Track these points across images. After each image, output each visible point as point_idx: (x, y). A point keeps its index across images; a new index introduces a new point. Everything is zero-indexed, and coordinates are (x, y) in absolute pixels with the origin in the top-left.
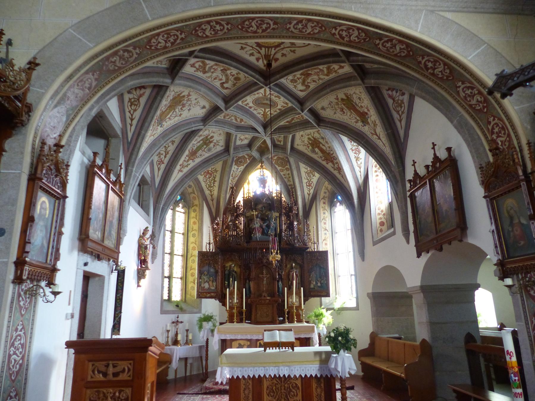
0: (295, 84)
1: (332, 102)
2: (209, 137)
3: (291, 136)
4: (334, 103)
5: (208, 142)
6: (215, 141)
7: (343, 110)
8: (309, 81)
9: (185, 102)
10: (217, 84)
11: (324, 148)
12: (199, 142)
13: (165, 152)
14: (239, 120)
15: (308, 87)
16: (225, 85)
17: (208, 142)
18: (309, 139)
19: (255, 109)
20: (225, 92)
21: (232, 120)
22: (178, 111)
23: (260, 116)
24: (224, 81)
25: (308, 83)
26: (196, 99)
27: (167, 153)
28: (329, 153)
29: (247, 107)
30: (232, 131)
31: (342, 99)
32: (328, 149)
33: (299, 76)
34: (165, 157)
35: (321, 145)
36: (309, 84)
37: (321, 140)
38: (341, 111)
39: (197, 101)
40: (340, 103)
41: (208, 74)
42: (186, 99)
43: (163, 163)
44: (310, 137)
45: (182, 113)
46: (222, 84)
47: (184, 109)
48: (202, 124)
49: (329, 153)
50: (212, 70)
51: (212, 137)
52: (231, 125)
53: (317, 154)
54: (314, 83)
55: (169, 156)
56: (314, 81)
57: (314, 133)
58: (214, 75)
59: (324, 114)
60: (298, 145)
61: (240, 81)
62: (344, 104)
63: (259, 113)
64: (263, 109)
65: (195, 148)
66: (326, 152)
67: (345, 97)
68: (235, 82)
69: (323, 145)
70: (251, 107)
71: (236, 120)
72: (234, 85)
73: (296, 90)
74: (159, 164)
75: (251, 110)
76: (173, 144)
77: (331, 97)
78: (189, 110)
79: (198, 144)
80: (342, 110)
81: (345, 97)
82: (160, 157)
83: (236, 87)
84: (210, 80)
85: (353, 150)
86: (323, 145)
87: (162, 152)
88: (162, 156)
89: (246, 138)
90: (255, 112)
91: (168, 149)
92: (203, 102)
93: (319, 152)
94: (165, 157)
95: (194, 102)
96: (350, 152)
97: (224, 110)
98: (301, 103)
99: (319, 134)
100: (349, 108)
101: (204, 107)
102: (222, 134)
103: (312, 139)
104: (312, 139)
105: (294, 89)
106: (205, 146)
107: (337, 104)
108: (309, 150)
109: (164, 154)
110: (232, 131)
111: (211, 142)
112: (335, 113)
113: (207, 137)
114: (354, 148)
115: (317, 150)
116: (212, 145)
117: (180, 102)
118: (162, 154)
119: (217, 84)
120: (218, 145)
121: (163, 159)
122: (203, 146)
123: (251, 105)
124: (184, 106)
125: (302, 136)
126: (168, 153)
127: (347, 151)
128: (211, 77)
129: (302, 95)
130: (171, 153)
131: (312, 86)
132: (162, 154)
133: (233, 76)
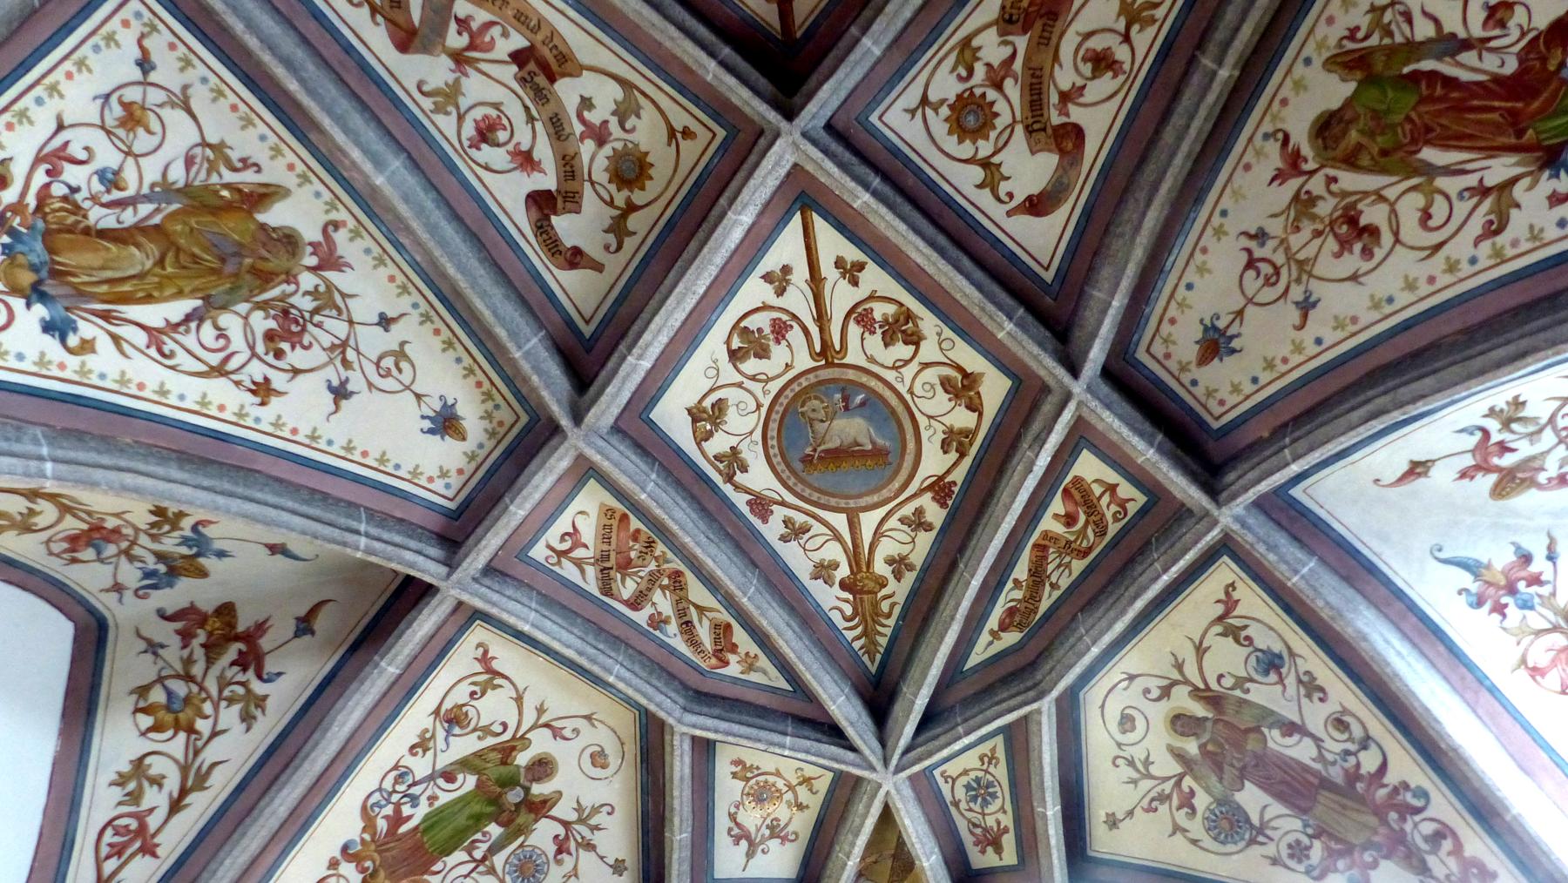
0: (985, 148)
1: (1261, 236)
2: (522, 759)
3: (1047, 706)
4: (1275, 227)
5: (514, 796)
6: (564, 810)
7: (1351, 219)
8: (1065, 78)
9: (307, 304)
10: (508, 193)
11: (1301, 751)
12: (449, 776)
13: (184, 769)
14: (704, 633)
15: (1069, 139)
16: (562, 224)
17: (514, 796)
18: (1180, 723)
19: (795, 532)
20: (578, 291)
21: (658, 621)
22: (238, 342)
23: (830, 599)
24: (547, 181)
25: (1065, 97)
26: (385, 322)
27: (193, 779)
28: (1354, 776)
29: (740, 501)
30: (666, 706)
31: (1327, 127)
32: (1334, 746)
33: (992, 49)
34: (176, 806)
35: (1276, 740)
36: (1076, 114)
37: (1263, 694)
38: (1345, 245)
39: (390, 340)
40: (1316, 185)
41: (436, 70)
42: (307, 281)
43: (149, 850)
44: (1182, 700)
45: (278, 380)
46: (542, 203)
47: (296, 357)
48: (434, 551)
49: (1354, 776)
50: (456, 40)
51: (543, 767)
52: (662, 668)
53: (1258, 833)
54: (1106, 84)
55: (201, 806)
56: (1102, 62)
57: (1200, 650)
58: (475, 88)
59: (1224, 391)
60: (1113, 822)
61: (653, 188)
62: (1350, 162)
63: (823, 571)
64: (840, 521)
65: (417, 814)
66: (1326, 784)
67: (1335, 91)
68: (620, 199)
69: (1290, 728)
70: (761, 505)
71: (687, 627)
72: (618, 228)
73: (998, 211)
74: (117, 850)
75: (772, 530)
76: (247, 719)
77: (1250, 192)
78: (340, 393)
79: (446, 795)
80: (1354, 230)
81: (1335, 91)
82: (135, 797)
83: (630, 244)
84: (447, 123)
85: (1536, 672)
86: (1290, 728)
87: (157, 766)
88: (157, 799)
89: (776, 831)
90: (797, 559)
91: (209, 755)
92: (443, 375)
93: (1276, 808)
94: (176, 806)
95: (373, 341)
96: (1515, 686)
97: (565, 422)
98: (1052, 308)
99: (1233, 633)
100: (1396, 158)
101: (446, 423)
102: (614, 761)
103: (1199, 710)
104: (1199, 710)
105: (984, 198)
106: (495, 830)
107: (1303, 204)
108: (1196, 827)
109: (173, 784)
110: (666, 706)
111: (540, 808)
112: (1306, 306)
113: (507, 752)
114: (1540, 653)
115: (1252, 798)
116: (543, 834)
117: (266, 278)
118: (157, 782)
119: (508, 193)
120: (590, 846)
121: (153, 822)
122: (478, 821)
123: (759, 477)
124: (288, 330)
125: (1127, 722)
126: (201, 782)
127: (1493, 691)
128: (448, 97)
129: (1041, 240)
130: (221, 784)
131: (1099, 117)
132: (157, 782)
133: (600, 136)
